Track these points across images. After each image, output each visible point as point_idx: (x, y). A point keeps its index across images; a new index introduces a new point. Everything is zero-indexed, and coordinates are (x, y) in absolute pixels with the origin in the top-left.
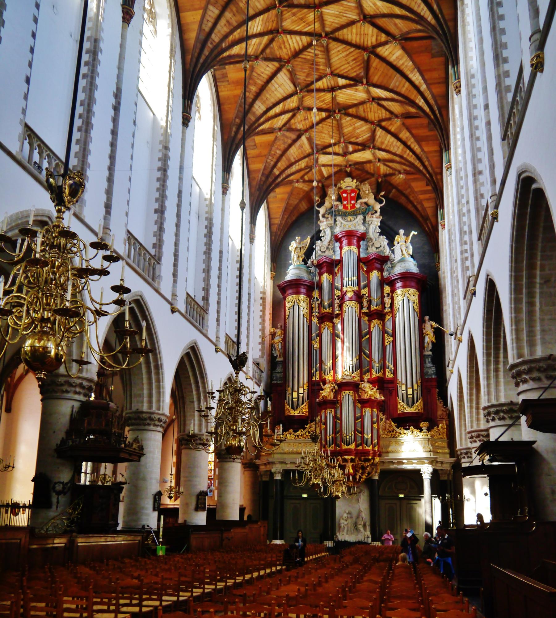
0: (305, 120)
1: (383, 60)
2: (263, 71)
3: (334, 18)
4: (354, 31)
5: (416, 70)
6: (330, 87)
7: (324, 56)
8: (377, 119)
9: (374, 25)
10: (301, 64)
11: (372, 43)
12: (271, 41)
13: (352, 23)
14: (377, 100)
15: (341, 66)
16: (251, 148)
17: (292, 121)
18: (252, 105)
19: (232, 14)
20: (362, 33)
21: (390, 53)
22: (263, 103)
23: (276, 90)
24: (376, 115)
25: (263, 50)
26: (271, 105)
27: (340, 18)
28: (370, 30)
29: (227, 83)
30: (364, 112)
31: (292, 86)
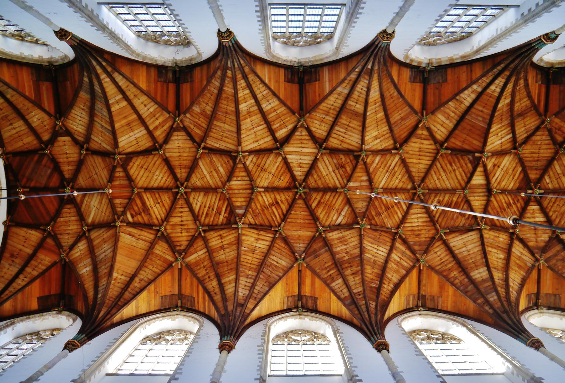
0: (535, 229)
1: (451, 133)
2: (439, 258)
3: (395, 178)
4: (414, 161)
5: (458, 98)
6: (486, 194)
7: (442, 195)
8: (552, 146)
9: (407, 140)
10: (445, 219)
11: (431, 145)
12: (405, 242)
13: (403, 161)
14: (515, 144)
15: (457, 179)
16: (558, 300)
17: (531, 244)
18: (472, 281)
19: (349, 268)
20: (418, 153)
21: (442, 126)
22: (477, 267)
23: (468, 251)
24: (544, 147)
25: (413, 252)
26: (484, 260)
27: (395, 173)
28: (414, 145)
29: (440, 299)
30: (538, 160)
31: (470, 234)
